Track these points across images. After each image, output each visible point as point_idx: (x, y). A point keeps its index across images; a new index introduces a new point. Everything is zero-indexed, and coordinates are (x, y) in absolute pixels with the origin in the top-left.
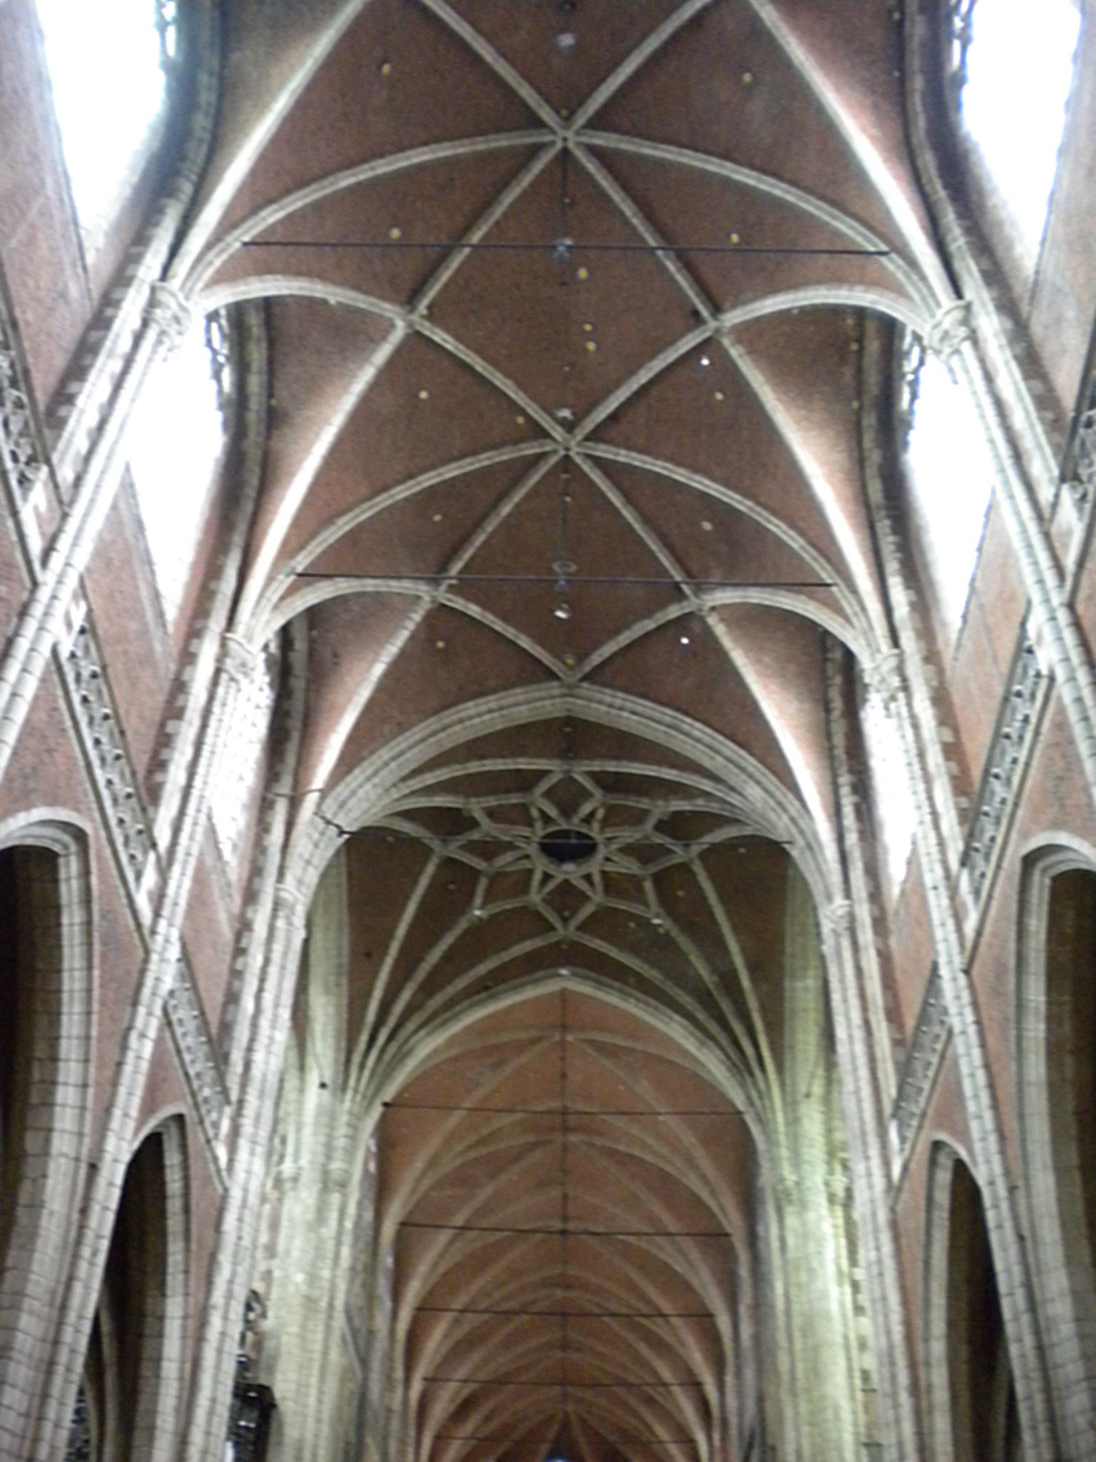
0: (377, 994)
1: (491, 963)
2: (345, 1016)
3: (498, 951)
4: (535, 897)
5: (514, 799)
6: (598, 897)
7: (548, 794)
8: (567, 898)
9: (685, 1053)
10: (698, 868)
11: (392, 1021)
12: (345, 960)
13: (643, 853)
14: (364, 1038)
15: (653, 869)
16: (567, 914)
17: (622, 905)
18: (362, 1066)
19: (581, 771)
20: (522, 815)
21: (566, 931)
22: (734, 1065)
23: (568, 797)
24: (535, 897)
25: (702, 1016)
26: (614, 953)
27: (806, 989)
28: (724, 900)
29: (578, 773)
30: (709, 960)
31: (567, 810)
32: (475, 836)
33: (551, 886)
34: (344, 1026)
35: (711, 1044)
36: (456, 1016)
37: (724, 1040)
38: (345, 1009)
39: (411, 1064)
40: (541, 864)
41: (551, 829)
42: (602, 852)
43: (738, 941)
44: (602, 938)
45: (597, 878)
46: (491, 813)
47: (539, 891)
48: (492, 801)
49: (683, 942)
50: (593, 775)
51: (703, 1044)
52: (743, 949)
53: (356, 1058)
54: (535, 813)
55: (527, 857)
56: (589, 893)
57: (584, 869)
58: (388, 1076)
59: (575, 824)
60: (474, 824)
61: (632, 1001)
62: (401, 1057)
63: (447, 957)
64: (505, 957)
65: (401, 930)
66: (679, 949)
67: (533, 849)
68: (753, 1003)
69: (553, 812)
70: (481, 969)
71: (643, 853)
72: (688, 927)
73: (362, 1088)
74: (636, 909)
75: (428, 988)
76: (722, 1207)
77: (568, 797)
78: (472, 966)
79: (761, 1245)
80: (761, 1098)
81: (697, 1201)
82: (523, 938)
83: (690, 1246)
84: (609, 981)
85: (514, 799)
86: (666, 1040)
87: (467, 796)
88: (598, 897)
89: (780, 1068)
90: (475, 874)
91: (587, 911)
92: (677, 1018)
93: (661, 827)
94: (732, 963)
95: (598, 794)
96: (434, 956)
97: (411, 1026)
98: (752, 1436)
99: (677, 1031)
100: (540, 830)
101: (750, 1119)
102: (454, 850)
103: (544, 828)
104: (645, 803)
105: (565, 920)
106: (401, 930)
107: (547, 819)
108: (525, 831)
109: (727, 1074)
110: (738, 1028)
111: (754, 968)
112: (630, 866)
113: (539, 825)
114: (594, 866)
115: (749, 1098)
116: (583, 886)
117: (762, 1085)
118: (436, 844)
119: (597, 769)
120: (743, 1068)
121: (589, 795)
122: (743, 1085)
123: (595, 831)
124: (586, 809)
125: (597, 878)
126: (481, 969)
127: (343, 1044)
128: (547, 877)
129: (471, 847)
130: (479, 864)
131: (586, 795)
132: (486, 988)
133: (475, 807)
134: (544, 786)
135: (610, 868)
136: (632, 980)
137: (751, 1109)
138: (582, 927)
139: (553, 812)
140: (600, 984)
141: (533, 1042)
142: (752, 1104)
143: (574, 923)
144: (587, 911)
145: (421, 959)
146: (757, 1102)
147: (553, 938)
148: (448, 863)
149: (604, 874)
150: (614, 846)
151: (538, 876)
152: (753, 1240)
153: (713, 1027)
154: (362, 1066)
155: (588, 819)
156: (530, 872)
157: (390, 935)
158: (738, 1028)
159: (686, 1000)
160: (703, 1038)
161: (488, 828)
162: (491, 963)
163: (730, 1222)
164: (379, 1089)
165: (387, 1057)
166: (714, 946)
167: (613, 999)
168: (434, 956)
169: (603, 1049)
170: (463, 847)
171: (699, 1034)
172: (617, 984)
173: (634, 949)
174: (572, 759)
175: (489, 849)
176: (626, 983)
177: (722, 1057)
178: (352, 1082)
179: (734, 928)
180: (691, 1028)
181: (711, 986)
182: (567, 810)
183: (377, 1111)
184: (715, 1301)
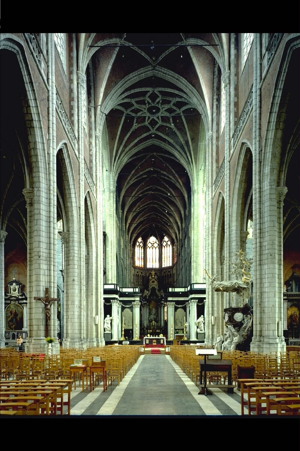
1: (138, 139)
3: (139, 137)
4: (146, 123)
5: (142, 99)
6: (160, 123)
7: (149, 97)
8: (153, 123)
17: (165, 124)
19: (157, 90)
21: (153, 131)
23: (153, 97)
24: (146, 123)
28: (187, 123)
29: (156, 91)
30: (183, 137)
31: (153, 101)
40: (148, 114)
42: (161, 111)
43: (189, 133)
44: (161, 132)
45: (160, 117)
46: (137, 102)
47: (148, 121)
48: (137, 99)
50: (158, 91)
54: (146, 102)
56: (158, 121)
60: (133, 105)
63: (128, 139)
64: (141, 138)
66: (177, 135)
67: (146, 111)
69: (150, 101)
70: (136, 141)
72: (179, 129)
74: (168, 125)
77: (153, 97)
78: (134, 140)
82: (144, 133)
85: (142, 99)
87: (131, 99)
88: (160, 123)
93: (174, 105)
94: (188, 138)
95: (160, 96)
96: (126, 139)
103: (148, 106)
104: (171, 99)
112: (167, 114)
113: (147, 105)
114: (160, 114)
116: (157, 120)
118: (125, 111)
119: (160, 90)
121: (158, 97)
124: (157, 100)
125: (160, 117)
126: (136, 141)
128: (149, 118)
129: (133, 111)
134: (148, 94)
136: (167, 142)
138: (157, 130)
139: (150, 101)
143: (155, 129)
145: (123, 139)
148: (128, 114)
149: (161, 117)
155: (158, 103)
156: (145, 117)
157: (117, 135)
161: (136, 106)
162: (138, 139)
168: (126, 139)
170: (131, 111)
173: (168, 135)
174: (154, 87)
175: (137, 111)
176: (166, 143)
179: (189, 130)
182: (153, 101)
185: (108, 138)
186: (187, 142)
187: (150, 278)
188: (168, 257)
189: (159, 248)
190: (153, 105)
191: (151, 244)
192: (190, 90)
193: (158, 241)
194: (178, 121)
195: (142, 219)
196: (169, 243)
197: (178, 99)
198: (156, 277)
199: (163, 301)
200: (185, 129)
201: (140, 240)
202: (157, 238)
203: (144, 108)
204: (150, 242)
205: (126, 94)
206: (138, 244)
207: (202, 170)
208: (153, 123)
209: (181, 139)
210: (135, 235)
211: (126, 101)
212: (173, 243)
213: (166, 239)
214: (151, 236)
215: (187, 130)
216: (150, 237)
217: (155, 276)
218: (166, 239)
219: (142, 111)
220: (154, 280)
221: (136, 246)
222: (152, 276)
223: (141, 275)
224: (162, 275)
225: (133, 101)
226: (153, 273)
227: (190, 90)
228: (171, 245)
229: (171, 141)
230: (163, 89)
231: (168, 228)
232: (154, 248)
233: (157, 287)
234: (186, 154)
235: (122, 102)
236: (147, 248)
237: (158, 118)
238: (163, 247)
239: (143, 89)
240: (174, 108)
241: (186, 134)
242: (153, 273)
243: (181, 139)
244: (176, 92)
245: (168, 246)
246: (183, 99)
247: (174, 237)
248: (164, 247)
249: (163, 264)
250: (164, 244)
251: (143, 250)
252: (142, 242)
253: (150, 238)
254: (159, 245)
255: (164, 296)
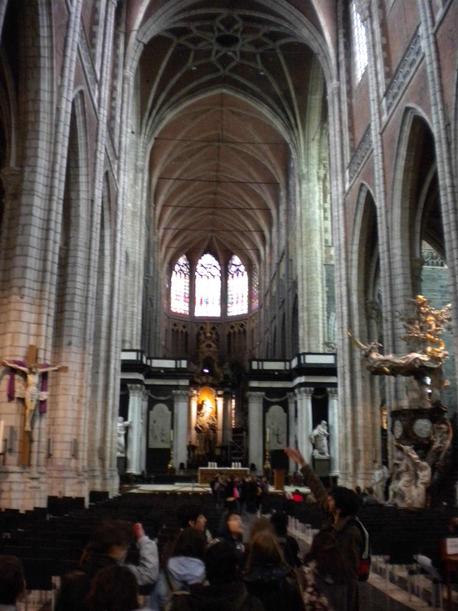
0: (152, 97)
2: (139, 105)
6: (237, 60)
8: (225, 60)
9: (267, 118)
10: (278, 51)
11: (157, 107)
12: (139, 83)
13: (257, 44)
14: (147, 114)
15: (260, 50)
16: (225, 65)
17: (247, 63)
18: (147, 124)
20: (211, 29)
21: (223, 72)
22: (286, 125)
24: (213, 58)
25: (275, 106)
26: (243, 81)
27: (316, 99)
28: (288, 64)
31: (228, 27)
32: (192, 36)
33: (220, 55)
34: (139, 110)
35: (278, 117)
36: (181, 104)
37: (283, 116)
38: (139, 103)
39: (165, 123)
40: (216, 47)
41: (221, 34)
42: (241, 42)
46: (198, 28)
48: (198, 24)
49: (271, 78)
51: (275, 117)
52: (293, 82)
53: (145, 121)
54: (215, 28)
55: (211, 44)
56: (235, 58)
57: (232, 49)
58: (156, 128)
59: (230, 33)
60: (191, 31)
61: (249, 98)
62: (161, 120)
63: (178, 82)
65: (161, 72)
67: (213, 41)
68: (295, 103)
69: (222, 27)
71: (257, 44)
73: (147, 133)
74: (252, 65)
75: (171, 94)
76: (276, 173)
77: (229, 23)
79: (291, 189)
80: (296, 139)
81: (266, 169)
83: (264, 187)
84: (239, 90)
85: (208, 23)
86: (260, 114)
88: (237, 60)
89: (304, 128)
90: (190, 51)
91: (233, 64)
92: (266, 106)
93: (265, 35)
96: (173, 81)
97: (164, 108)
98: (283, 254)
99: (265, 111)
100: (217, 34)
101: (291, 146)
102: (182, 40)
104: (260, 26)
105: (224, 67)
106: (161, 72)
107: (219, 30)
108: (210, 34)
109: (284, 129)
110: (289, 113)
111: (297, 89)
112: (251, 49)
114: (237, 48)
115: (291, 139)
117: (296, 134)
118: (175, 40)
120: (290, 127)
122: (289, 134)
123: (239, 35)
124: (236, 27)
125: (238, 53)
127: (139, 116)
128: (218, 52)
130: (191, 46)
131: (235, 21)
132: (192, 93)
133: (192, 26)
134: (220, 18)
135: (244, 49)
137: (292, 143)
140: (237, 92)
141: (208, 110)
142: (292, 141)
144: (233, 64)
146: (295, 141)
147: (219, 74)
148: (180, 45)
150: (246, 41)
151: (214, 53)
152: (287, 186)
153: (280, 111)
154: (147, 124)
158: (289, 113)
159: (270, 100)
160: (275, 114)
163: (279, 179)
164: (153, 132)
165: (156, 121)
166: (281, 80)
167: (240, 97)
168: (173, 81)
169: (233, 113)
171: (273, 112)
172: (243, 92)
175: (196, 41)
177: (282, 122)
178: (143, 131)
179: (291, 74)
180: (271, 110)
181: (280, 96)
182: (228, 27)
183: (152, 141)
184: (271, 205)
185: (139, 80)
186: (287, 94)
187: (202, 337)
188: (240, 296)
189: (221, 278)
190: (227, 33)
191: (205, 268)
192: (296, 17)
193: (220, 265)
194: (271, 59)
195: (190, 220)
196: (242, 268)
197: (273, 29)
198: (214, 336)
199: (229, 387)
200: (284, 74)
201: (182, 260)
202: (217, 259)
203: (211, 38)
204: (202, 266)
205: (182, 16)
206: (177, 268)
207: (316, 141)
208: (225, 60)
209: (276, 88)
210: (172, 251)
211: (178, 25)
212: (250, 269)
213: (236, 260)
214: (205, 252)
215: (287, 74)
216: (203, 255)
217: (211, 333)
218: (236, 260)
219: (204, 40)
220: (209, 342)
221: (174, 273)
222: (205, 333)
223: (182, 332)
224: (226, 333)
225: (192, 26)
226: (208, 328)
227: (296, 17)
228: (245, 273)
229: (257, 89)
230: (248, 13)
231: (241, 239)
232: (211, 277)
233: (215, 358)
234: (284, 111)
235: (172, 26)
236: (196, 276)
237: (235, 53)
238: (230, 276)
239: (213, 11)
240: (266, 40)
241: (285, 80)
242: (208, 328)
243: (276, 88)
244: (271, 18)
245: (240, 274)
246: (282, 28)
247: (254, 257)
248: (233, 277)
249: (229, 310)
250: (233, 269)
251: (188, 281)
252: (186, 265)
253: (202, 258)
254: (221, 272)
255: (230, 376)
